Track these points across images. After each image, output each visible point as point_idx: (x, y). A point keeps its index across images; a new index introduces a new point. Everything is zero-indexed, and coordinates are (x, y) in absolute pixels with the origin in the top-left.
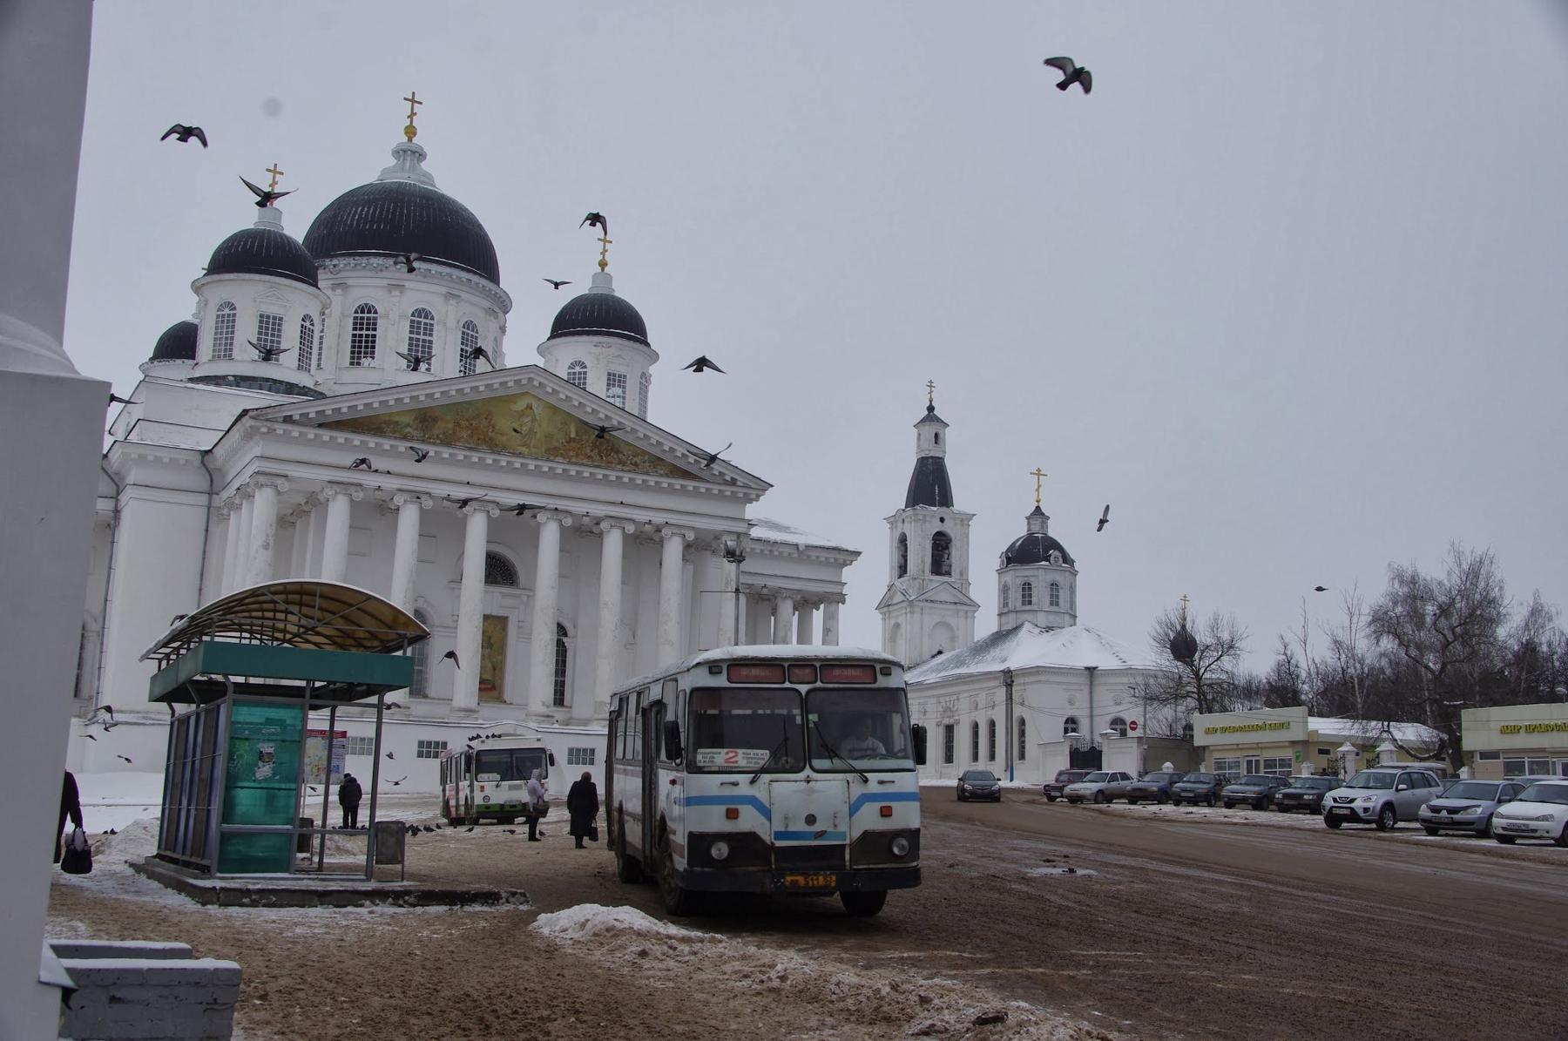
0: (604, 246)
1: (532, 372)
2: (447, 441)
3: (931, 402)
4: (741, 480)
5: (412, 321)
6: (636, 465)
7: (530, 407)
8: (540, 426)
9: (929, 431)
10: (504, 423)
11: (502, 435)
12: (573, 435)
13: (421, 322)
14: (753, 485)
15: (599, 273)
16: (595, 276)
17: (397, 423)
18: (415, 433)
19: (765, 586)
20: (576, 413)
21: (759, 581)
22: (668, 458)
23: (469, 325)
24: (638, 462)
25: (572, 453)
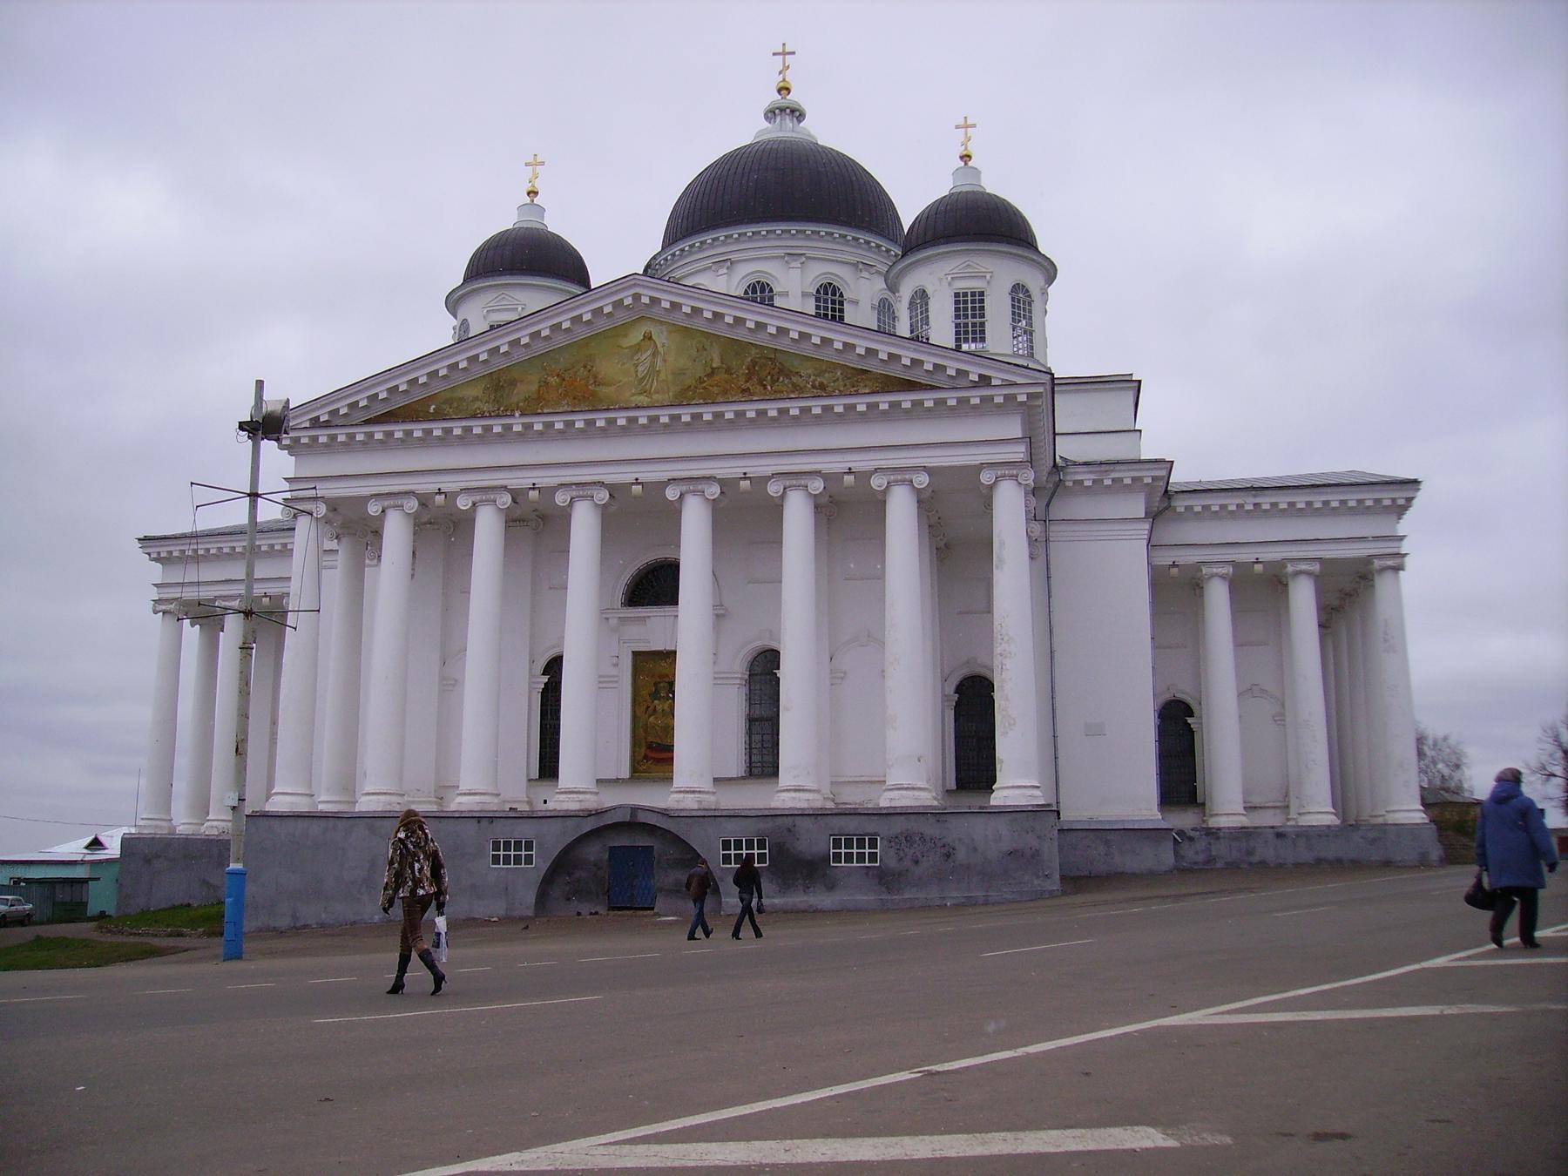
0: (966, 134)
1: (635, 285)
2: (531, 407)
4: (997, 377)
6: (822, 387)
8: (665, 361)
10: (608, 367)
11: (609, 385)
12: (714, 365)
14: (1020, 381)
15: (961, 168)
17: (462, 399)
19: (1257, 562)
21: (1246, 555)
22: (872, 366)
24: (825, 382)
25: (716, 390)
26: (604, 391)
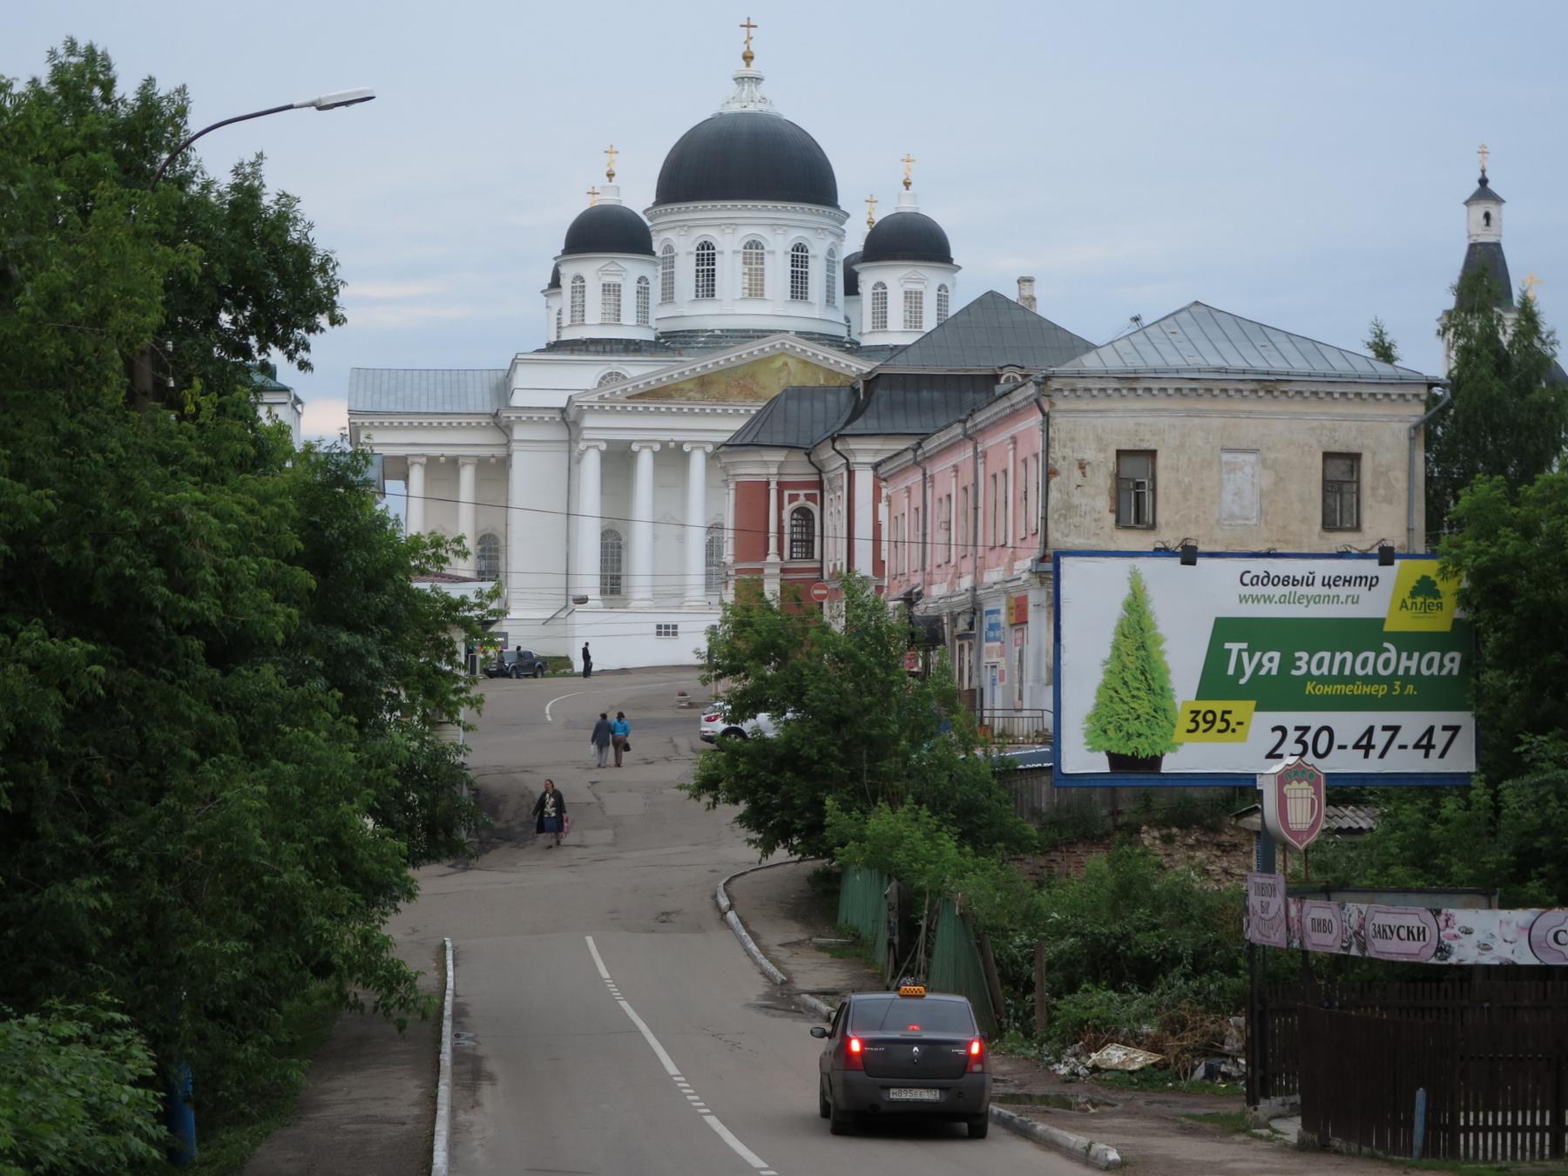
2: (722, 399)
3: (1483, 171)
5: (745, 254)
7: (786, 364)
9: (1478, 211)
17: (682, 390)
18: (698, 396)
20: (824, 364)
23: (800, 248)
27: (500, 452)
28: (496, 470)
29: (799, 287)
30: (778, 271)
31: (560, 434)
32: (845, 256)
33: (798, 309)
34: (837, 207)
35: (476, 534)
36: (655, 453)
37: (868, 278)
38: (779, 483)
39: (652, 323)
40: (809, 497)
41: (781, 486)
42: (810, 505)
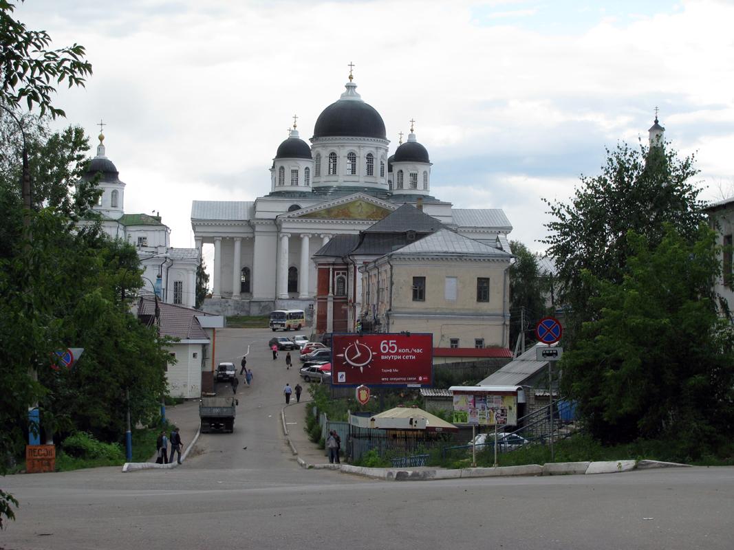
2: (336, 217)
10: (352, 210)
13: (352, 157)
16: (410, 135)
26: (352, 215)
27: (250, 235)
28: (248, 243)
29: (370, 171)
30: (362, 164)
31: (274, 229)
32: (388, 157)
33: (370, 179)
34: (385, 139)
35: (241, 267)
36: (310, 239)
37: (396, 169)
38: (333, 269)
39: (311, 185)
40: (344, 274)
41: (334, 270)
42: (344, 276)
